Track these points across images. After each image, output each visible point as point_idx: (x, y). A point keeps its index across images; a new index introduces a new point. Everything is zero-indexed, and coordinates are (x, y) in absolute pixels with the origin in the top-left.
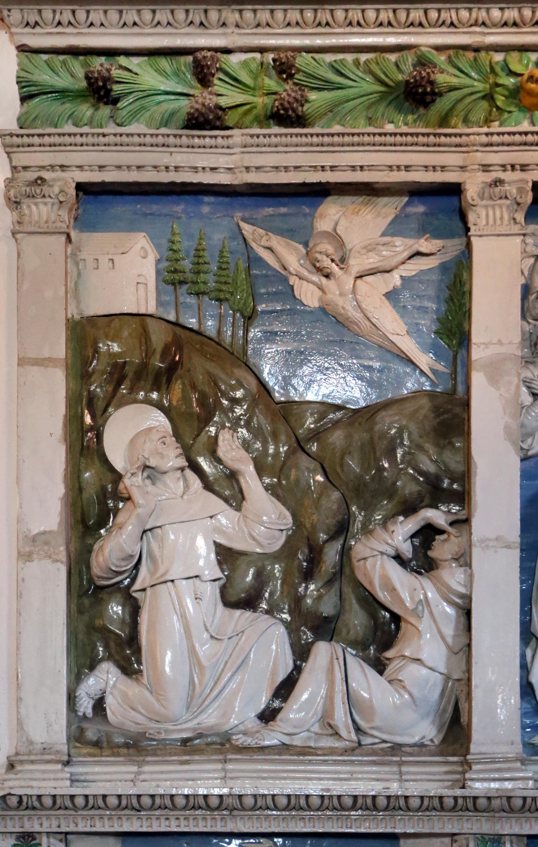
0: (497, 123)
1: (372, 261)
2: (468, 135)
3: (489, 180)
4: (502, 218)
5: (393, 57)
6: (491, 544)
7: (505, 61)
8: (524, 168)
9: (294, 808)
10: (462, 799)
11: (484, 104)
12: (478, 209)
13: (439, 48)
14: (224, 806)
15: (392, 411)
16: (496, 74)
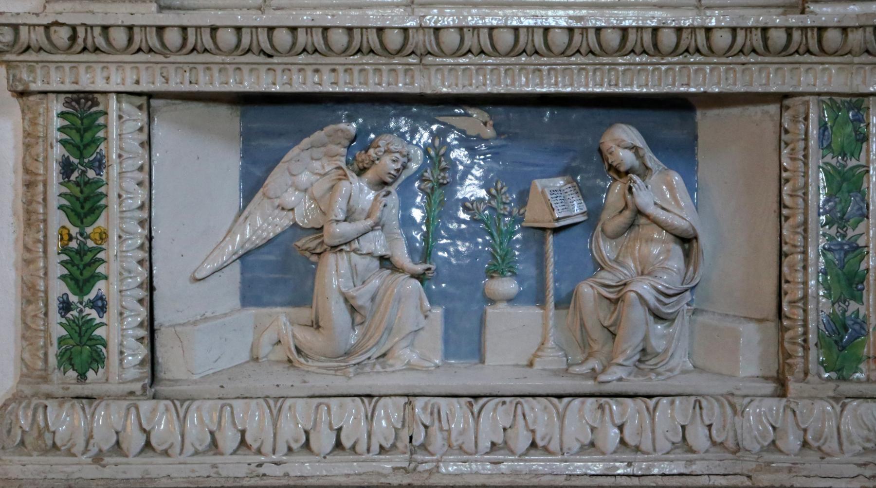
9: (524, 51)
10: (800, 32)
14: (409, 48)
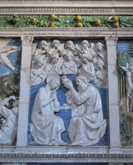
0: (27, 27)
1: (4, 50)
2: (22, 29)
3: (25, 36)
4: (28, 43)
5: (9, 16)
6: (23, 103)
7: (29, 17)
8: (32, 34)
11: (25, 24)
12: (23, 41)
13: (17, 15)
15: (6, 77)
16: (27, 19)
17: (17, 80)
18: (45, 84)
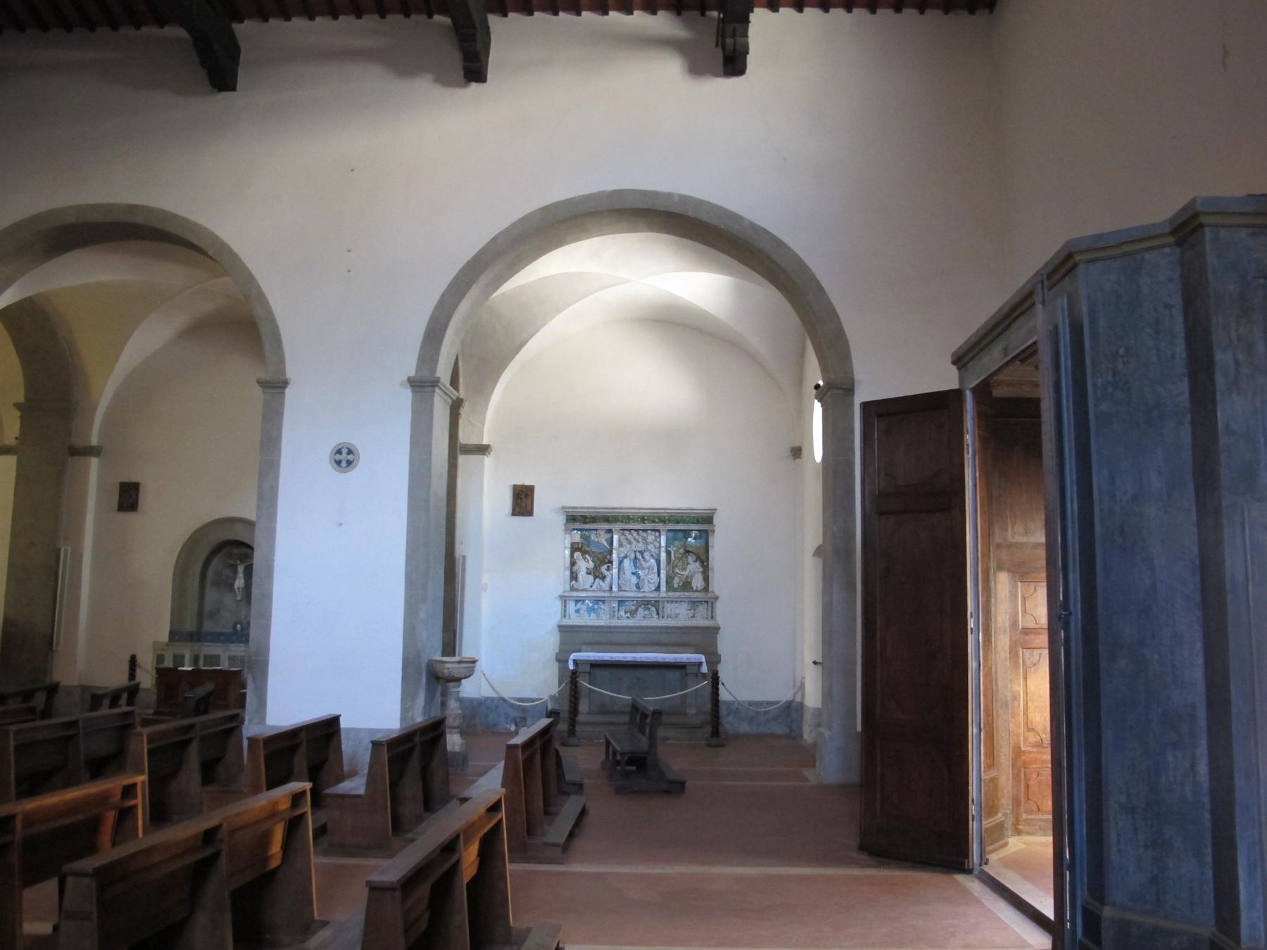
17: (611, 553)
18: (626, 557)
